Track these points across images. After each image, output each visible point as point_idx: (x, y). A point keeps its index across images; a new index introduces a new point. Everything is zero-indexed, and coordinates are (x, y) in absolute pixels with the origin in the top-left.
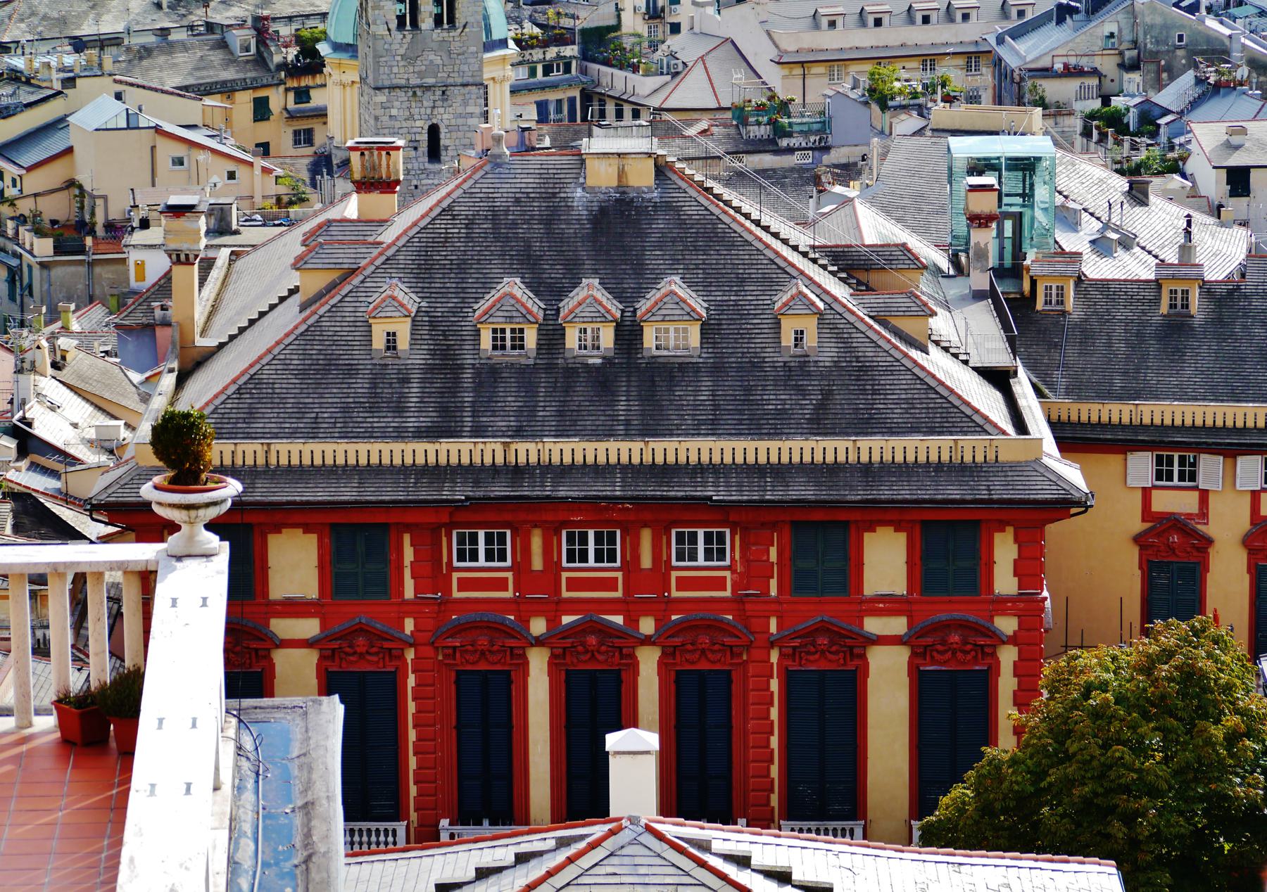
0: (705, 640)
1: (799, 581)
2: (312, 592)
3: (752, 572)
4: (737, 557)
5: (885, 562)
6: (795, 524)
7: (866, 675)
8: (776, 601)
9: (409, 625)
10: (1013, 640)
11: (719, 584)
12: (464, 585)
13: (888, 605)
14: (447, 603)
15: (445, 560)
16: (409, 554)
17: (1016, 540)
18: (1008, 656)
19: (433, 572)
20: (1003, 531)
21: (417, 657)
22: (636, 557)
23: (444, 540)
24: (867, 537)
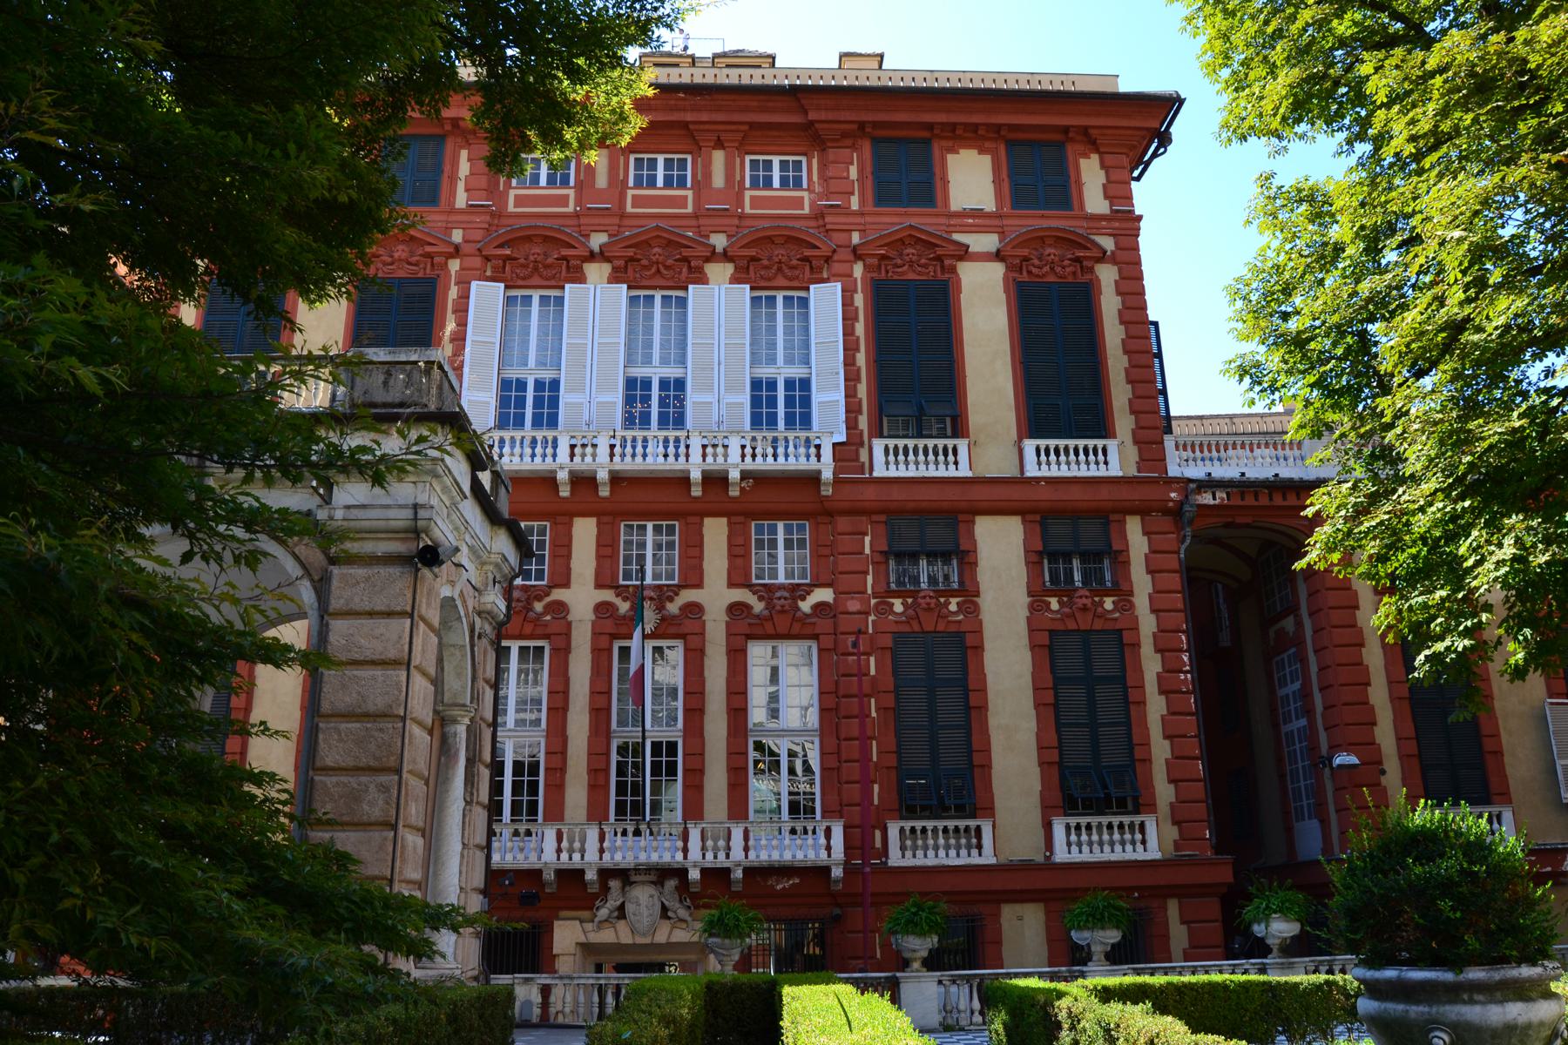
0: (780, 253)
1: (885, 192)
4: (815, 178)
5: (970, 179)
6: (876, 141)
8: (861, 214)
11: (798, 202)
12: (520, 201)
13: (977, 219)
14: (499, 215)
16: (464, 168)
17: (1103, 166)
18: (1107, 275)
21: (462, 269)
22: (708, 175)
24: (950, 157)
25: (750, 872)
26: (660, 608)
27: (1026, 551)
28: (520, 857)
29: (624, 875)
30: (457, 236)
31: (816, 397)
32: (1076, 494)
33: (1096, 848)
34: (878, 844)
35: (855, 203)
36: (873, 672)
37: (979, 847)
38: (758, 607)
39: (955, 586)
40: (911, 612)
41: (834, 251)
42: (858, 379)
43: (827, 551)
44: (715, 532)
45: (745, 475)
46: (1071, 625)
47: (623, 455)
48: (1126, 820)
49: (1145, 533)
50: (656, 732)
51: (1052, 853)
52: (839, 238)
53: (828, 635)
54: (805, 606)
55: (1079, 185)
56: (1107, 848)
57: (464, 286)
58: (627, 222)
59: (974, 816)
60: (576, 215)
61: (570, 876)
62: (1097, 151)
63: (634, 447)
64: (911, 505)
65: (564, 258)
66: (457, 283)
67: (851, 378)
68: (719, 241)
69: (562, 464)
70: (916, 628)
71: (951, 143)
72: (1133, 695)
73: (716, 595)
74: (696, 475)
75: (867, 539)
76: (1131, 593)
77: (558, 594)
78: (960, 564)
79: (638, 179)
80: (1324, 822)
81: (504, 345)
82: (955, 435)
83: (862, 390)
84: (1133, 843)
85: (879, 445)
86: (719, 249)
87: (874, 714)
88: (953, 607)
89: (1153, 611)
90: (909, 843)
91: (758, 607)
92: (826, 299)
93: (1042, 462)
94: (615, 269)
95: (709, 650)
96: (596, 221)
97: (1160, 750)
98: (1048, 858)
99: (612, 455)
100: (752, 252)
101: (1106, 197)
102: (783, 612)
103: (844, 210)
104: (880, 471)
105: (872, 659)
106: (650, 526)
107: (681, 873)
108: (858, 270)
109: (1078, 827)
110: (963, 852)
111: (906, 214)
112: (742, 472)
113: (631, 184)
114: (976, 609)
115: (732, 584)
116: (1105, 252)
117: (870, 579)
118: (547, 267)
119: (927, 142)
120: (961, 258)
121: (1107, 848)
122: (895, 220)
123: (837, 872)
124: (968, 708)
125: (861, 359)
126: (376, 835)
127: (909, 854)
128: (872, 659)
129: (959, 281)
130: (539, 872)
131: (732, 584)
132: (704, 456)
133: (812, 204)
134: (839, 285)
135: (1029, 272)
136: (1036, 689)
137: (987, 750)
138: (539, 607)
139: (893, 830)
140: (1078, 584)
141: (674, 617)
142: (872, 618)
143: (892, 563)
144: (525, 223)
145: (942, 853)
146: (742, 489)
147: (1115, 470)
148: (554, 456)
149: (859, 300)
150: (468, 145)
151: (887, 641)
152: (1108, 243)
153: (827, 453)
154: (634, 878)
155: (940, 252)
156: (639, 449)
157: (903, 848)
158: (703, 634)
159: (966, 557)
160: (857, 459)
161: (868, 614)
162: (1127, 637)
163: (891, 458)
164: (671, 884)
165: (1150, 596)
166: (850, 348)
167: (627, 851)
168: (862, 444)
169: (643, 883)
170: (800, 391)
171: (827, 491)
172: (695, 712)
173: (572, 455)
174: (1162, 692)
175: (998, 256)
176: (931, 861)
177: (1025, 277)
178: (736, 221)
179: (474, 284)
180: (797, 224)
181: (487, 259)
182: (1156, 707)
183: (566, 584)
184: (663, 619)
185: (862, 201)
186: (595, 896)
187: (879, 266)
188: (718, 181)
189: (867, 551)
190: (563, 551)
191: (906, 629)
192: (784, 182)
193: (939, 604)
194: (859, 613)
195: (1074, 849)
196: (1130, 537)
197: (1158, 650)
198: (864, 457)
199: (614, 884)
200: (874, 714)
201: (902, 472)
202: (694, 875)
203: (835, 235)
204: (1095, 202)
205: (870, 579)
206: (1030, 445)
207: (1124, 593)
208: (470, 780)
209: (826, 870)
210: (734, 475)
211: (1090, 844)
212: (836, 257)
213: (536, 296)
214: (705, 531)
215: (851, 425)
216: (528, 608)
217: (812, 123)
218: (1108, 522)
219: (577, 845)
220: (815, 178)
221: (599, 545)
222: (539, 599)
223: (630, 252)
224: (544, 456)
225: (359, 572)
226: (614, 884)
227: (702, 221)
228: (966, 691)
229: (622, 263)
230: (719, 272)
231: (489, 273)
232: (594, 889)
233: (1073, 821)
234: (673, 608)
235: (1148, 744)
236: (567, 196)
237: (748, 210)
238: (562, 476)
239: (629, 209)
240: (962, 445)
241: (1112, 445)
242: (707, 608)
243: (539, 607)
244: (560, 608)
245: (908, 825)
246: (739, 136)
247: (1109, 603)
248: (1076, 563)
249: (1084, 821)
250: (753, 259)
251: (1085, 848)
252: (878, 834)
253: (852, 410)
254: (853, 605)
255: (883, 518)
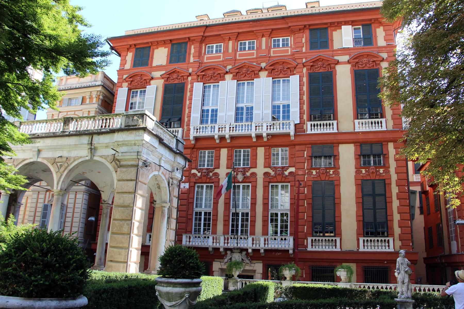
1: (313, 45)
2: (164, 63)
3: (297, 44)
4: (292, 43)
6: (311, 30)
7: (336, 74)
9: (190, 70)
10: (386, 60)
11: (287, 51)
12: (208, 58)
15: (203, 52)
16: (193, 51)
17: (384, 30)
19: (200, 54)
20: (379, 27)
23: (204, 47)
24: (334, 33)
25: (266, 251)
26: (244, 174)
27: (355, 155)
28: (203, 244)
29: (231, 250)
30: (190, 70)
31: (291, 110)
32: (371, 136)
33: (373, 247)
34: (305, 244)
35: (304, 50)
36: (306, 192)
37: (336, 246)
38: (273, 173)
39: (333, 166)
40: (318, 174)
41: (297, 65)
42: (304, 104)
43: (293, 156)
44: (261, 151)
45: (268, 135)
46: (368, 178)
47: (233, 130)
48: (383, 239)
49: (394, 148)
50: (241, 210)
51: (359, 248)
52: (299, 61)
53: (295, 182)
54: (286, 173)
55: (376, 37)
56: (376, 248)
57: (192, 84)
58: (236, 62)
59: (334, 236)
60: (223, 61)
61: (216, 250)
62: (382, 25)
63: (248, 127)
64: (318, 142)
65: (219, 74)
66: (190, 83)
67: (301, 103)
68: (263, 65)
69: (216, 134)
70: (319, 179)
71: (334, 28)
72: (388, 200)
73: (260, 170)
74: (253, 135)
75: (305, 152)
76: (389, 167)
77: (216, 171)
78: (334, 159)
79: (241, 48)
80: (457, 242)
81: (203, 100)
82: (334, 120)
83: (305, 107)
84: (385, 246)
85: (309, 123)
86: (263, 68)
87: (306, 205)
88: (331, 173)
89: (396, 173)
90: (314, 244)
91: (273, 173)
92: (294, 80)
93: (364, 126)
94: (234, 76)
95: (258, 186)
96: (228, 62)
97: (396, 217)
98: (358, 250)
99: (230, 130)
100: (272, 67)
101: (385, 40)
102: (279, 175)
103: (301, 52)
104: (309, 132)
105: (306, 189)
106: (242, 150)
107: (246, 250)
108: (305, 70)
109: (367, 241)
110: (331, 247)
111: (319, 52)
112: (267, 134)
113: (239, 50)
114: (338, 173)
115: (265, 167)
116: (383, 59)
117: (306, 164)
118: (216, 76)
119: (326, 28)
120: (336, 64)
121: (376, 248)
122: (315, 54)
123: (291, 252)
124: (335, 204)
125: (305, 98)
126: (126, 236)
127: (314, 247)
128: (306, 189)
129: (336, 71)
130: (208, 248)
131: (265, 167)
132: (256, 129)
133: (291, 51)
134: (298, 76)
135: (358, 67)
136: (356, 198)
137: (340, 216)
138: (211, 174)
139: (310, 239)
140: (372, 165)
141: (248, 177)
142: (306, 176)
143: (313, 159)
144: (208, 65)
145: (324, 247)
146: (268, 139)
147: (384, 129)
148: (214, 131)
149: (305, 79)
150: (193, 44)
151: (310, 183)
152: (385, 55)
153: (292, 127)
154: (234, 251)
155: (329, 62)
156: (241, 128)
157: (312, 245)
158: (256, 181)
159: (336, 157)
160: (303, 128)
161: (305, 175)
162: (387, 182)
163: (313, 127)
164: (244, 253)
165: (395, 168)
166: (301, 95)
167: (232, 244)
168: (304, 124)
169: (236, 252)
170: (287, 107)
171: (292, 138)
172: (254, 204)
173: (219, 131)
174: (398, 199)
175: (349, 62)
176: (320, 249)
177: (357, 68)
178: (268, 59)
179: (195, 83)
180: (285, 58)
181: (198, 76)
182: (396, 203)
183: (218, 168)
184: (245, 177)
185: (306, 49)
186: (224, 256)
187: (311, 69)
188: (264, 47)
189: (305, 156)
190: (218, 158)
191: (315, 179)
192: (283, 45)
193: (326, 172)
194: (302, 175)
195: (366, 247)
196: (389, 149)
197: (397, 186)
198: (305, 128)
199: (229, 252)
200: (306, 205)
201: (316, 132)
202: (250, 251)
203: (297, 60)
204: (381, 42)
205: (306, 164)
206: (357, 121)
207: (386, 167)
208: (168, 222)
209: (288, 251)
210: (264, 135)
211: (371, 246)
212: (298, 67)
213: (212, 85)
214: (258, 151)
215: (301, 118)
216: (208, 174)
217: (290, 27)
218: (382, 145)
219: (218, 241)
220: (292, 43)
221: (228, 156)
222: (211, 172)
223: (237, 71)
224: (211, 131)
225: (124, 169)
226: (229, 252)
227: (258, 60)
228: (334, 198)
229: (235, 74)
230: (263, 74)
231: (199, 80)
232: (223, 253)
233: (366, 239)
234: (248, 174)
235: (392, 215)
236: (220, 56)
237: (272, 55)
238: (216, 137)
239: (238, 58)
240: (335, 122)
241: (383, 120)
242: (258, 173)
243: (211, 174)
244: (216, 175)
245: (314, 238)
246: (269, 33)
247: (381, 171)
248: (372, 158)
249: (369, 239)
250: (273, 70)
251: (369, 247)
252: (305, 241)
253: (301, 113)
254: (300, 172)
255: (310, 146)
